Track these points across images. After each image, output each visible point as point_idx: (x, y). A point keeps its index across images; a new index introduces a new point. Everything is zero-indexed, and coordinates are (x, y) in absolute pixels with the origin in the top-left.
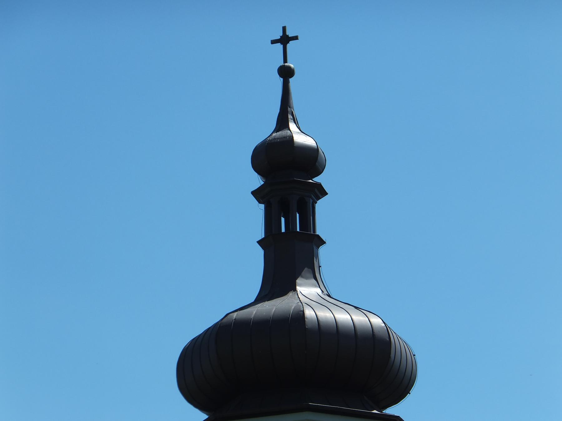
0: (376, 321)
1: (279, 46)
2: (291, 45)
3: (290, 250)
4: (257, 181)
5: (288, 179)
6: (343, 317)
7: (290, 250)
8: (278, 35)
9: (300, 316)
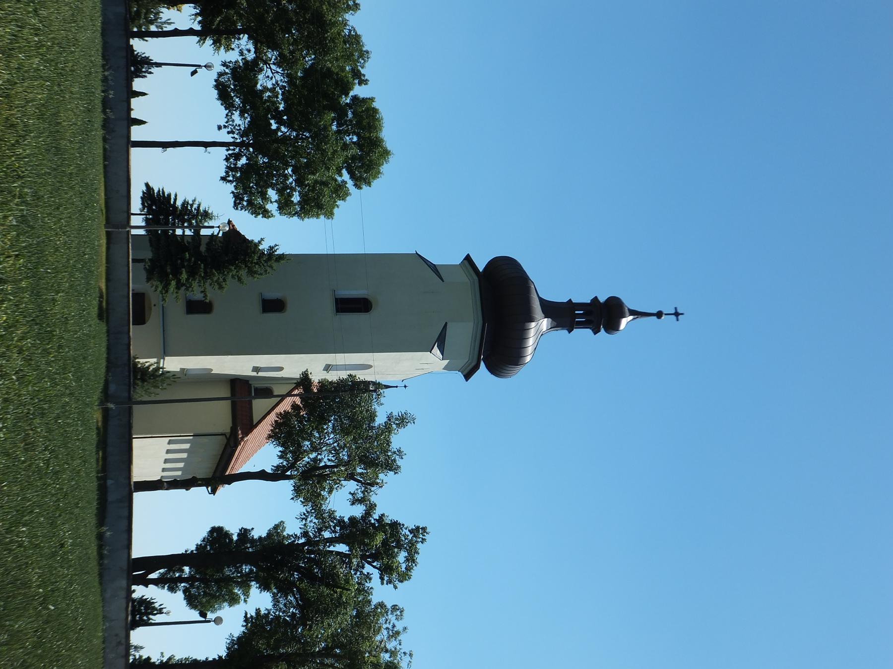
0: (528, 359)
2: (674, 317)
3: (565, 315)
4: (602, 299)
5: (603, 315)
6: (531, 342)
7: (565, 315)
8: (680, 311)
9: (531, 319)
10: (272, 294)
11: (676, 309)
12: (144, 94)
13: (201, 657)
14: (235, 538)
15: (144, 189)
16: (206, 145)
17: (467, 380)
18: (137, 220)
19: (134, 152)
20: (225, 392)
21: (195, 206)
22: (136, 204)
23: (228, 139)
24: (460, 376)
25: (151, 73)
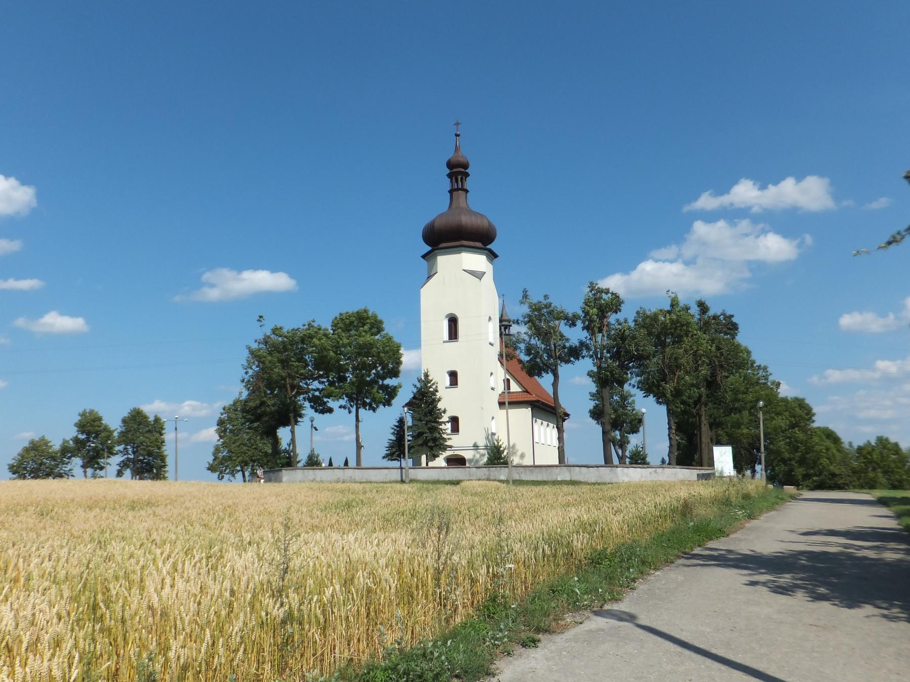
5: (458, 171)
10: (448, 378)
22: (396, 464)
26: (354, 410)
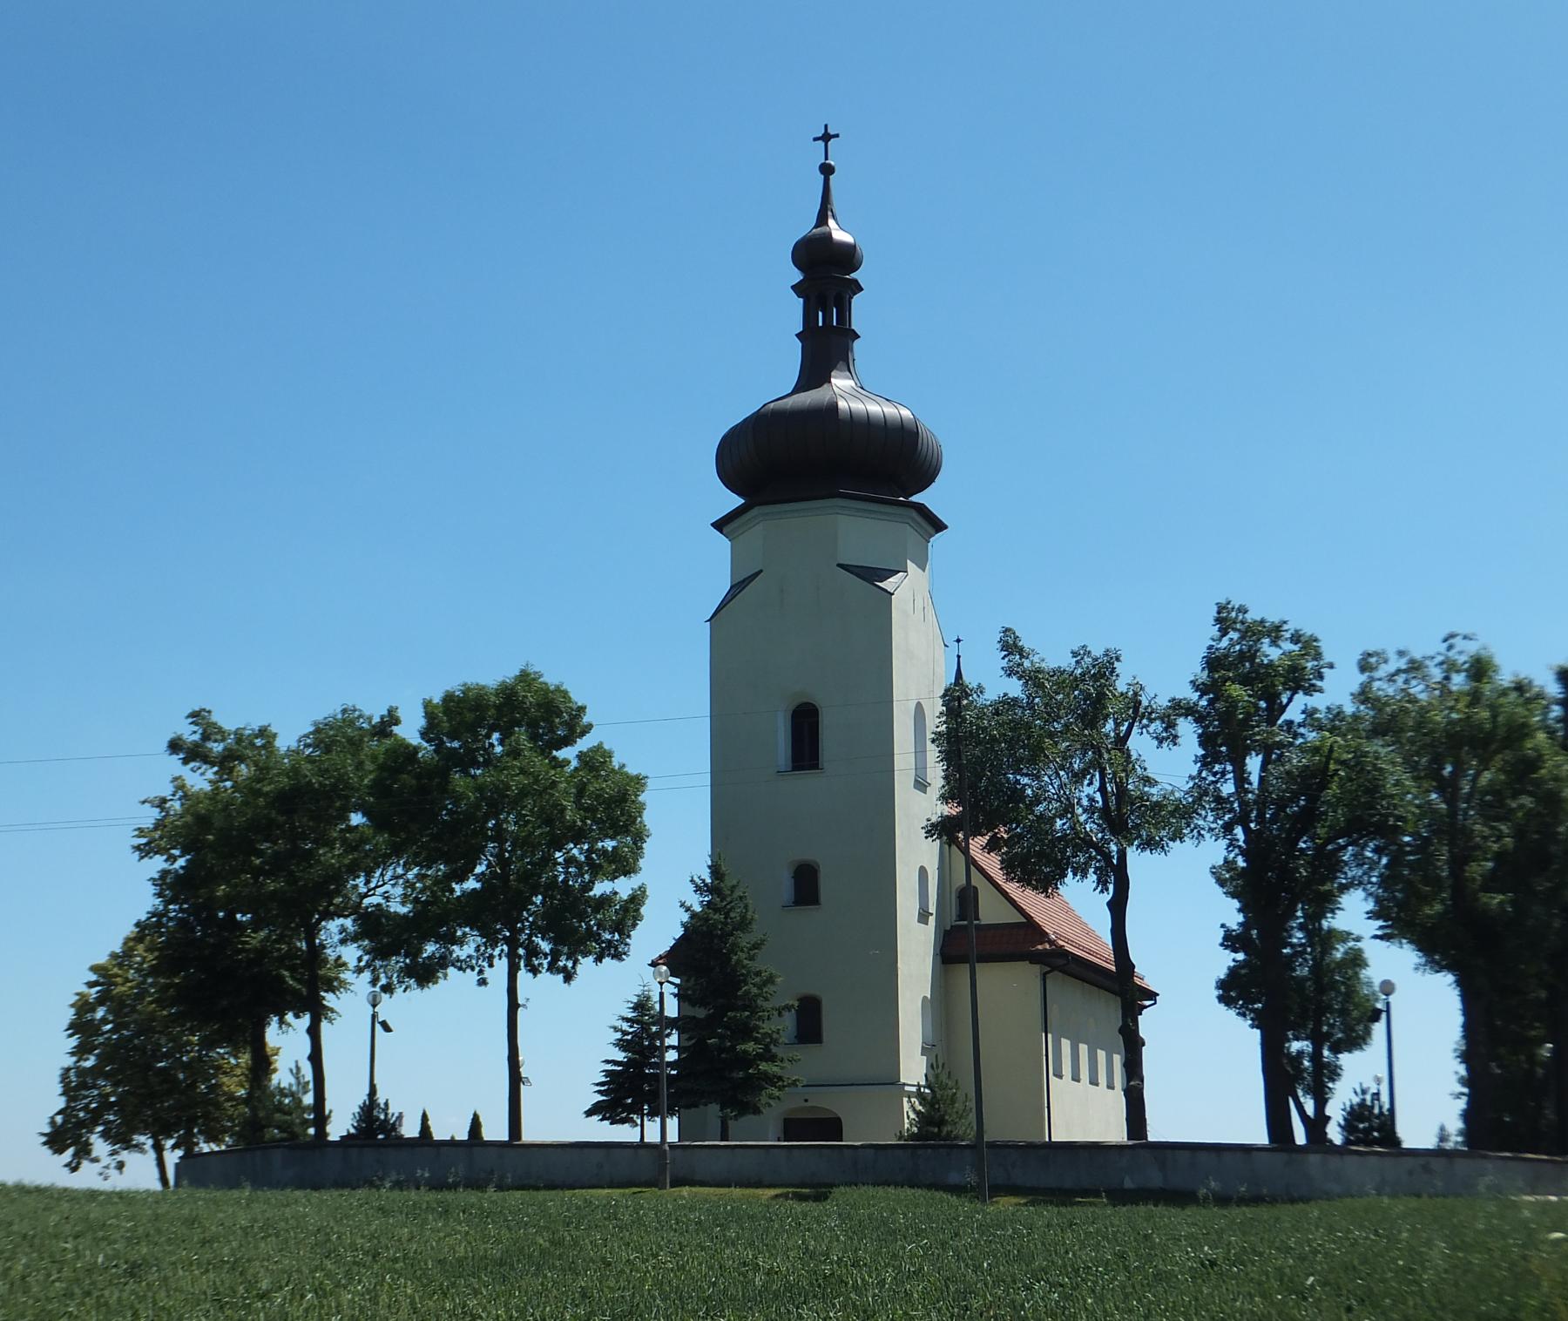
0: (906, 413)
1: (821, 144)
2: (832, 142)
3: (826, 345)
4: (797, 276)
5: (826, 274)
6: (874, 409)
7: (826, 345)
9: (833, 408)
10: (785, 887)
11: (816, 139)
12: (425, 1118)
13: (1460, 1019)
14: (1240, 956)
15: (596, 1118)
16: (513, 1006)
17: (946, 527)
18: (652, 1132)
19: (529, 1135)
20: (963, 971)
21: (625, 1026)
22: (625, 1133)
23: (502, 965)
24: (938, 540)
25: (386, 1104)
26: (498, 972)
